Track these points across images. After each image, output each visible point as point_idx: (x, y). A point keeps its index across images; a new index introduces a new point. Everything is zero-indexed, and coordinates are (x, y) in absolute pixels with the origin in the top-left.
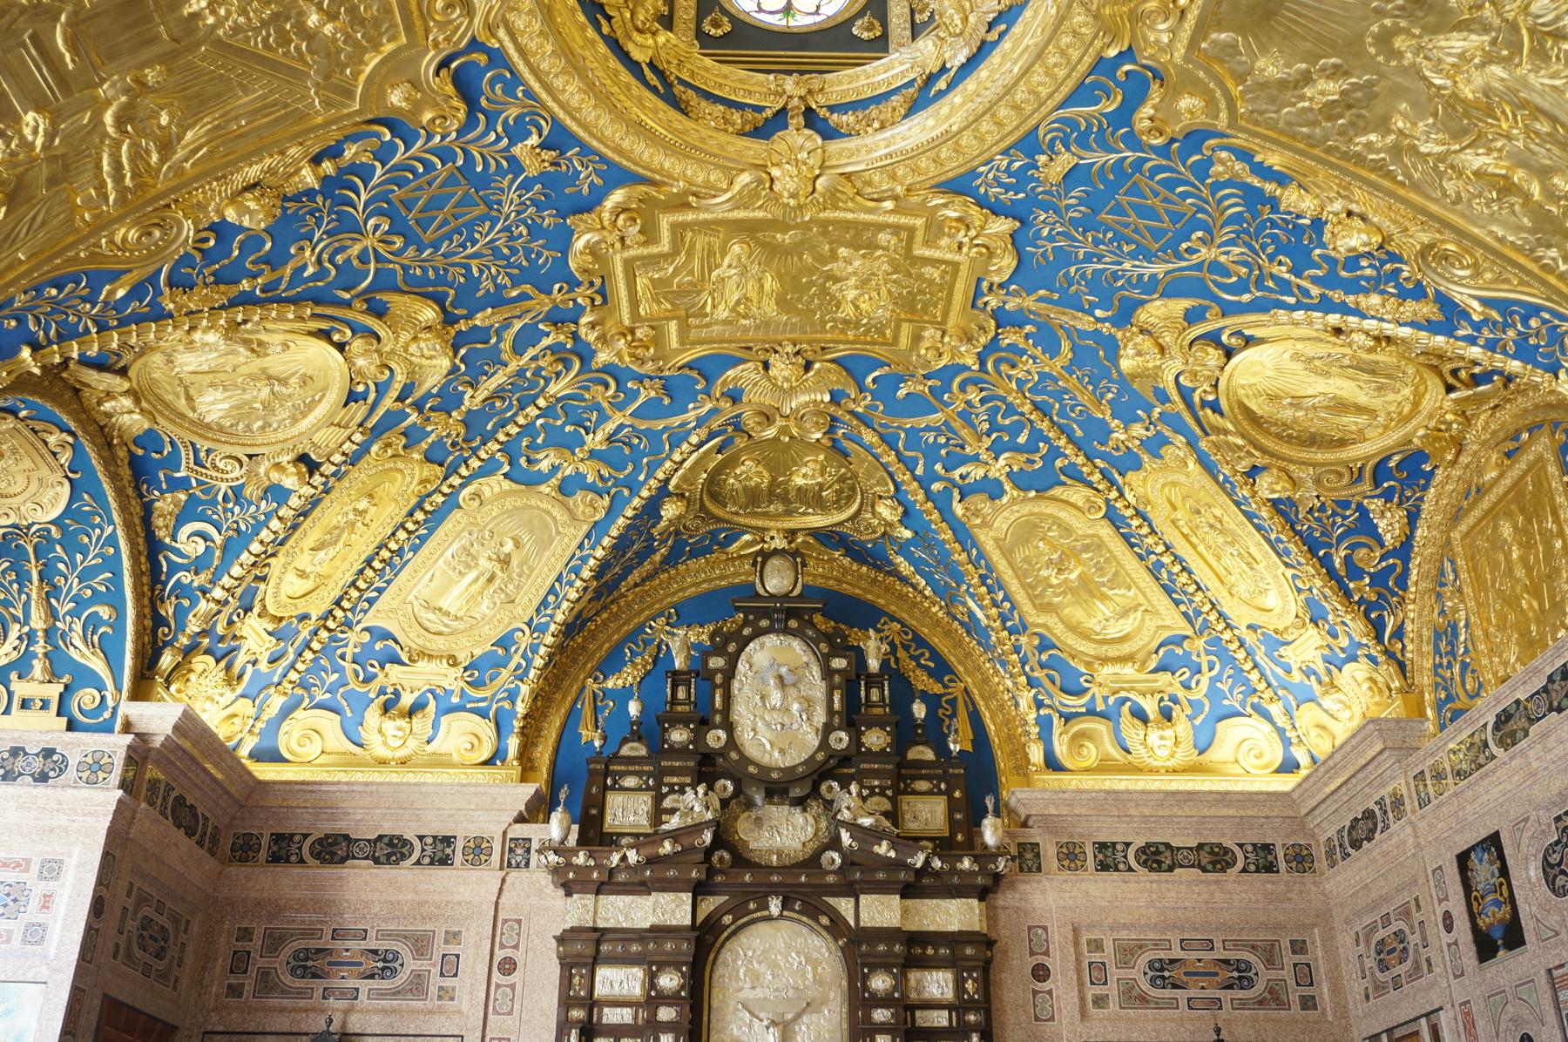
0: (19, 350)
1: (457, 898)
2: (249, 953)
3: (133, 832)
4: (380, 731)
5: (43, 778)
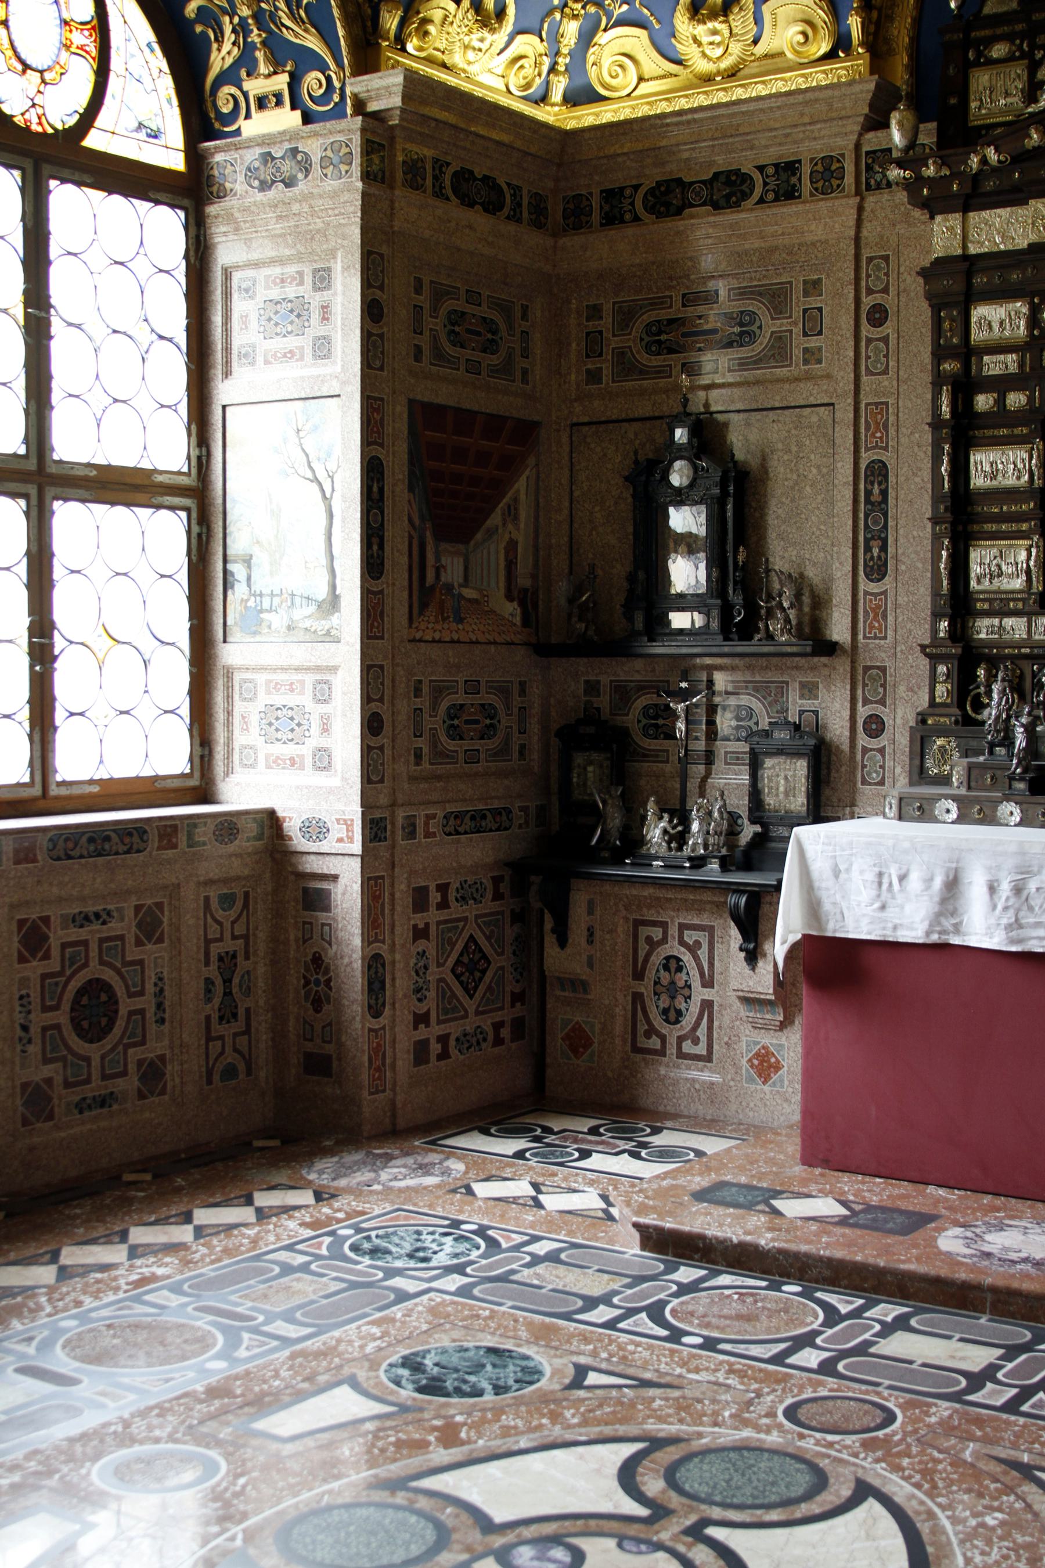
1: (809, 238)
2: (601, 333)
3: (397, 225)
4: (695, 40)
5: (289, 183)
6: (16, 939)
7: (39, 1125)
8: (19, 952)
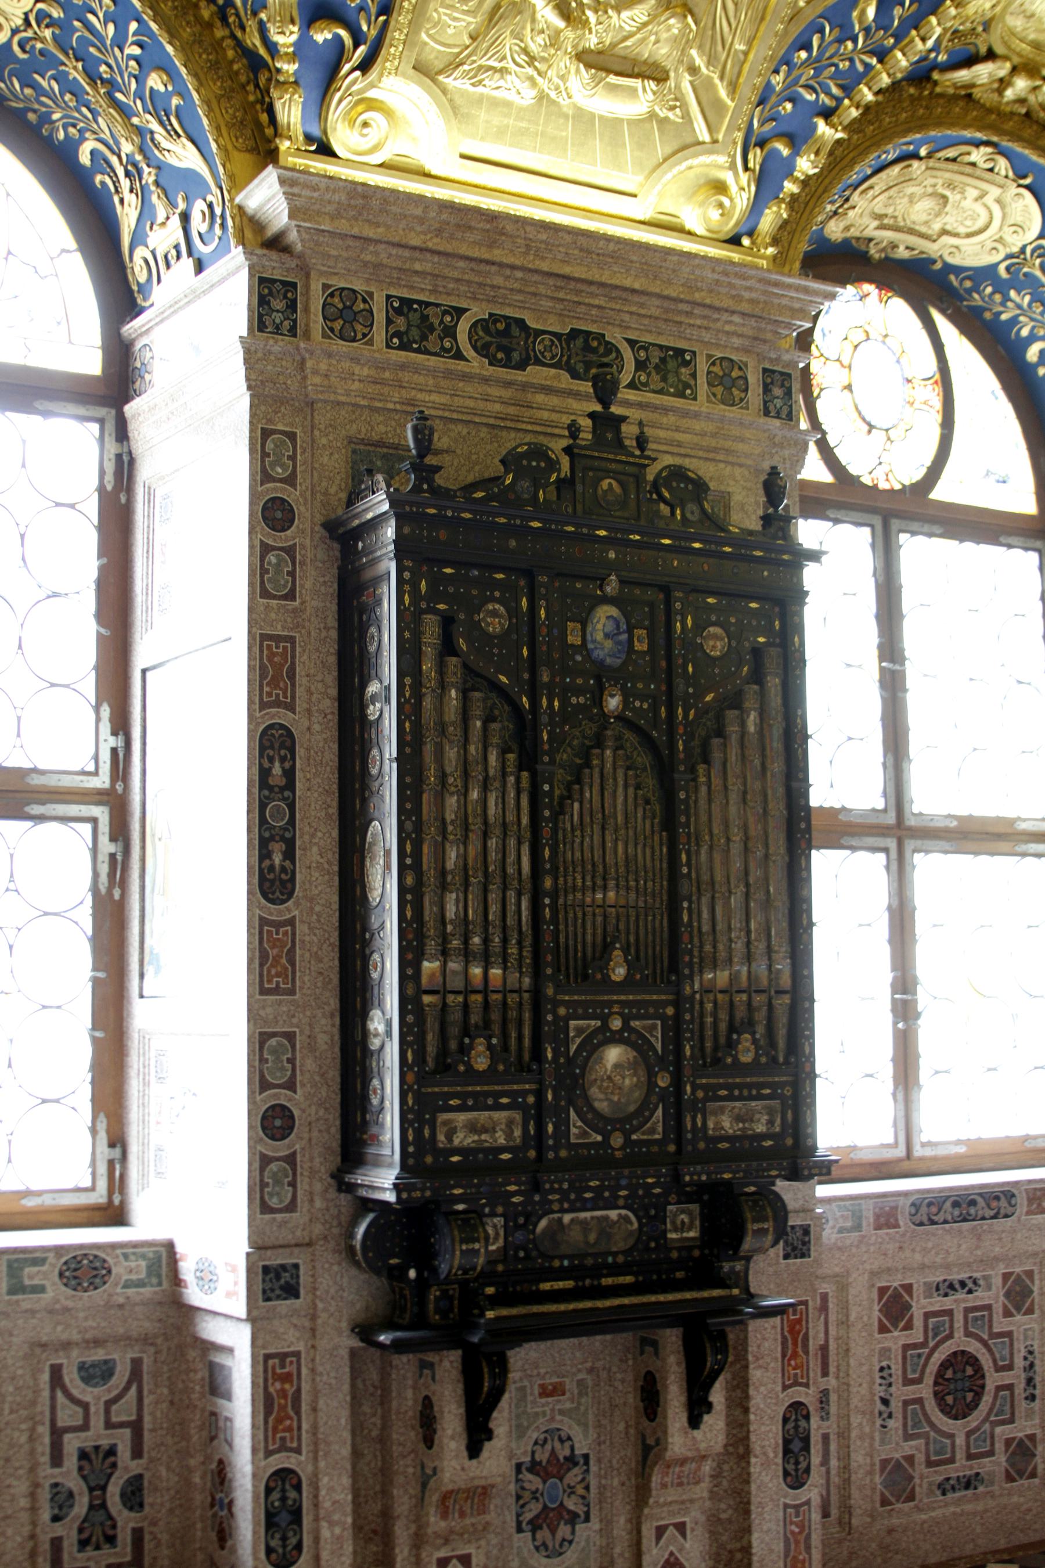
0: (814, 127)
6: (876, 1308)
7: (899, 1506)
8: (880, 1321)
